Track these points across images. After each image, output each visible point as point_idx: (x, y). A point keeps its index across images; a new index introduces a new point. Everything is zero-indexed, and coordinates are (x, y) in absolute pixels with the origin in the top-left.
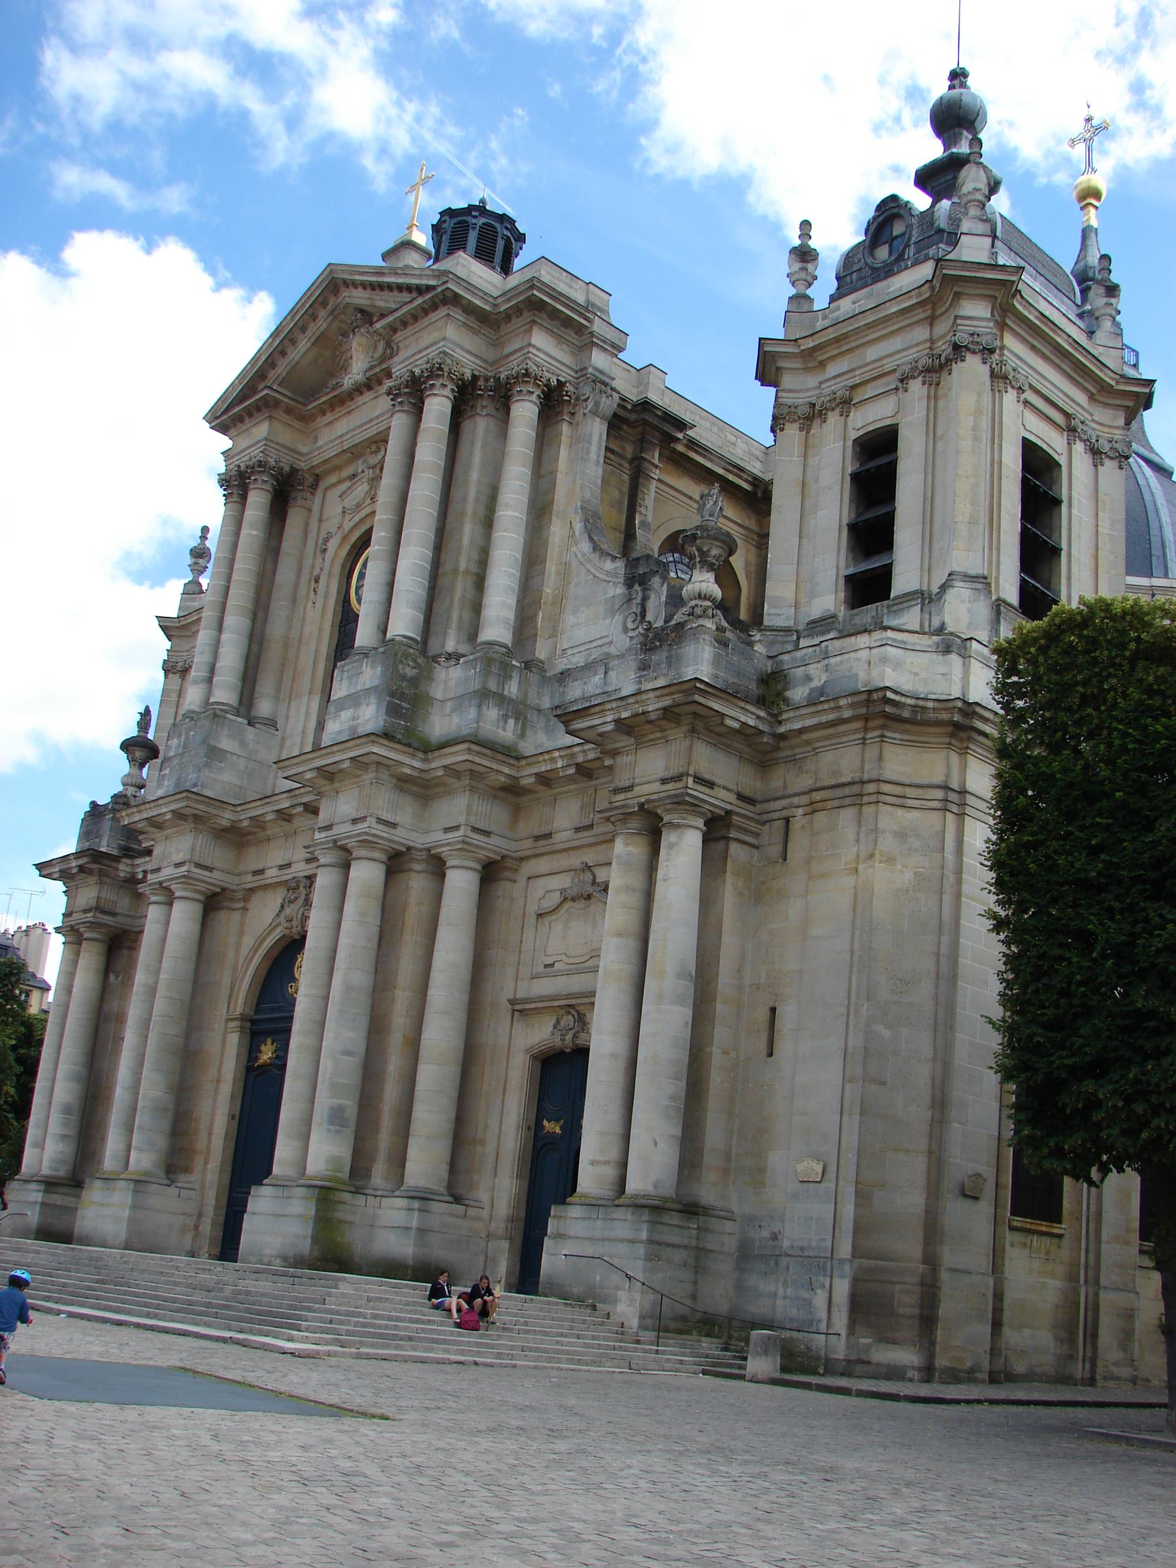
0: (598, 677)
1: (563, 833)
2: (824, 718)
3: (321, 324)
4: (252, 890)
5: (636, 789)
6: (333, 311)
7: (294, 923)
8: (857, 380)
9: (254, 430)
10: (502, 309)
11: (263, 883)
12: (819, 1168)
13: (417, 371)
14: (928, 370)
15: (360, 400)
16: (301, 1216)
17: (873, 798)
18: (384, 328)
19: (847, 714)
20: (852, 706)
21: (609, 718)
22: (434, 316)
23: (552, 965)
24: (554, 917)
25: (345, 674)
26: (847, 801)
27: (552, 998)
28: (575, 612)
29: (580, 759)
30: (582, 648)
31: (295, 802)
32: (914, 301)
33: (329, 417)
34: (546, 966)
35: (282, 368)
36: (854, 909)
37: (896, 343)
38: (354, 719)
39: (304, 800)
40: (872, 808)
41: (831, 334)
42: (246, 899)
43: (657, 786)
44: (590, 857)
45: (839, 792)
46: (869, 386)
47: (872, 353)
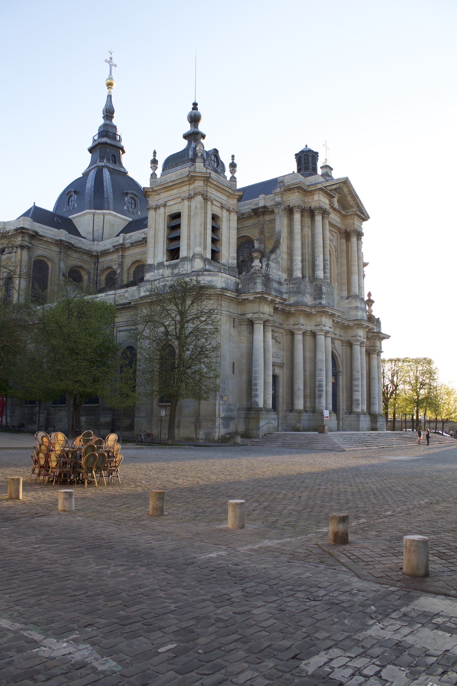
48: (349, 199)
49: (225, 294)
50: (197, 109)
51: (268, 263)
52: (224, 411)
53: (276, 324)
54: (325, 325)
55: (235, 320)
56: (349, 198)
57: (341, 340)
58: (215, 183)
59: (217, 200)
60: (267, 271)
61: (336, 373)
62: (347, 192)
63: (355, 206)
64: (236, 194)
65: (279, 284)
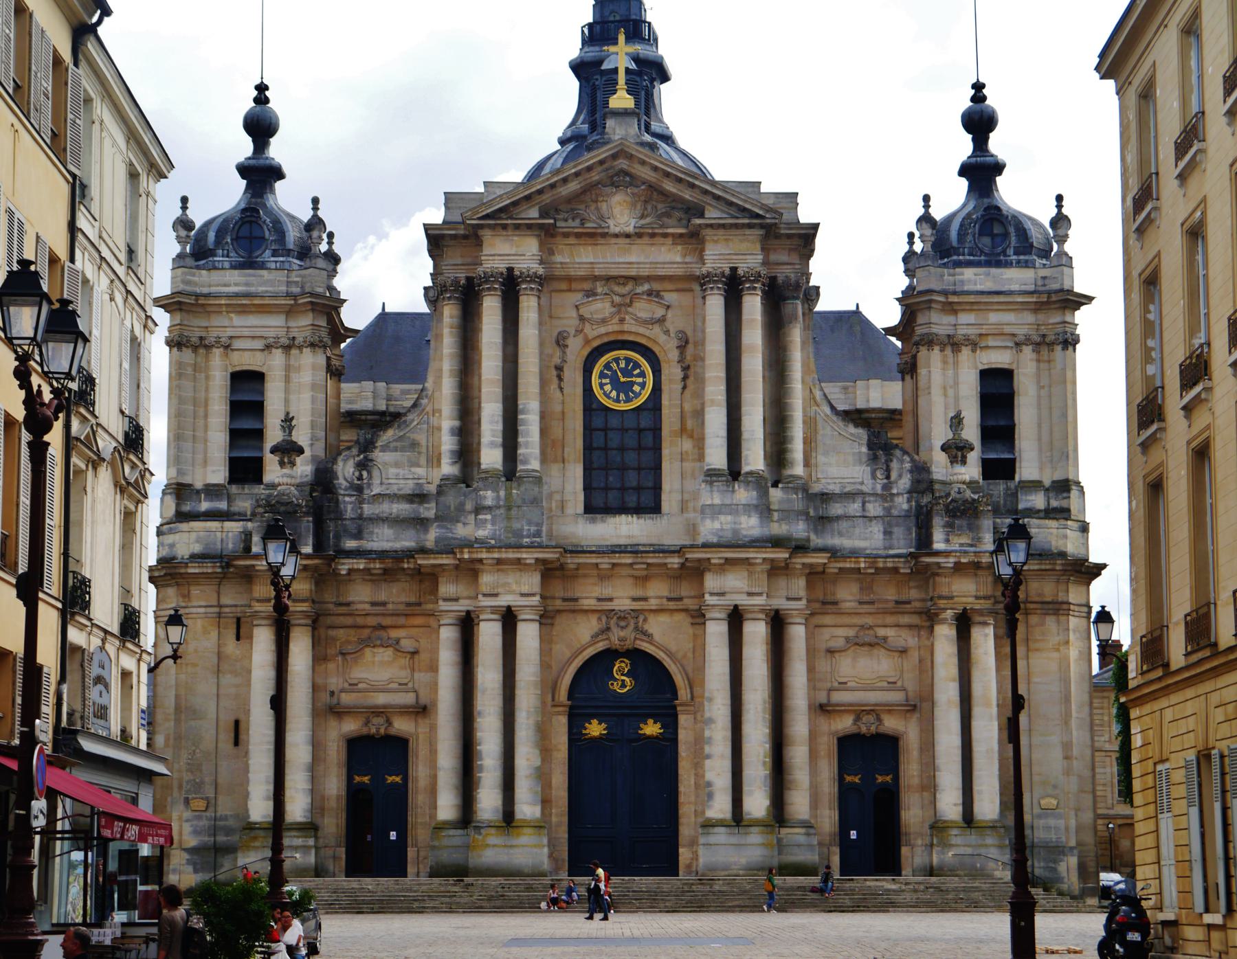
0: (856, 505)
1: (848, 604)
2: (1043, 567)
3: (595, 176)
4: (559, 611)
5: (956, 599)
6: (607, 170)
7: (628, 642)
8: (984, 332)
9: (515, 238)
10: (782, 232)
11: (576, 608)
12: (1055, 802)
13: (740, 272)
14: (1038, 344)
15: (613, 241)
16: (763, 844)
17: (1066, 612)
18: (700, 225)
19: (1058, 568)
20: (1062, 564)
21: (952, 560)
22: (748, 232)
23: (846, 683)
24: (843, 654)
25: (715, 489)
26: (1051, 612)
27: (851, 705)
28: (826, 453)
29: (881, 565)
30: (837, 481)
31: (639, 560)
32: (1034, 300)
33: (572, 240)
34: (840, 683)
35: (547, 198)
36: (1060, 670)
37: (1009, 317)
38: (735, 523)
39: (649, 561)
40: (1065, 617)
41: (972, 299)
42: (552, 618)
43: (971, 600)
44: (869, 620)
45: (1046, 606)
46: (990, 338)
47: (993, 317)
48: (674, 190)
49: (183, 571)
50: (267, 101)
51: (365, 458)
52: (196, 832)
53: (390, 606)
54: (496, 591)
55: (242, 620)
56: (669, 187)
57: (686, 610)
58: (223, 302)
59: (246, 334)
60: (360, 478)
61: (675, 707)
62: (652, 174)
63: (708, 199)
64: (301, 301)
65: (411, 502)
